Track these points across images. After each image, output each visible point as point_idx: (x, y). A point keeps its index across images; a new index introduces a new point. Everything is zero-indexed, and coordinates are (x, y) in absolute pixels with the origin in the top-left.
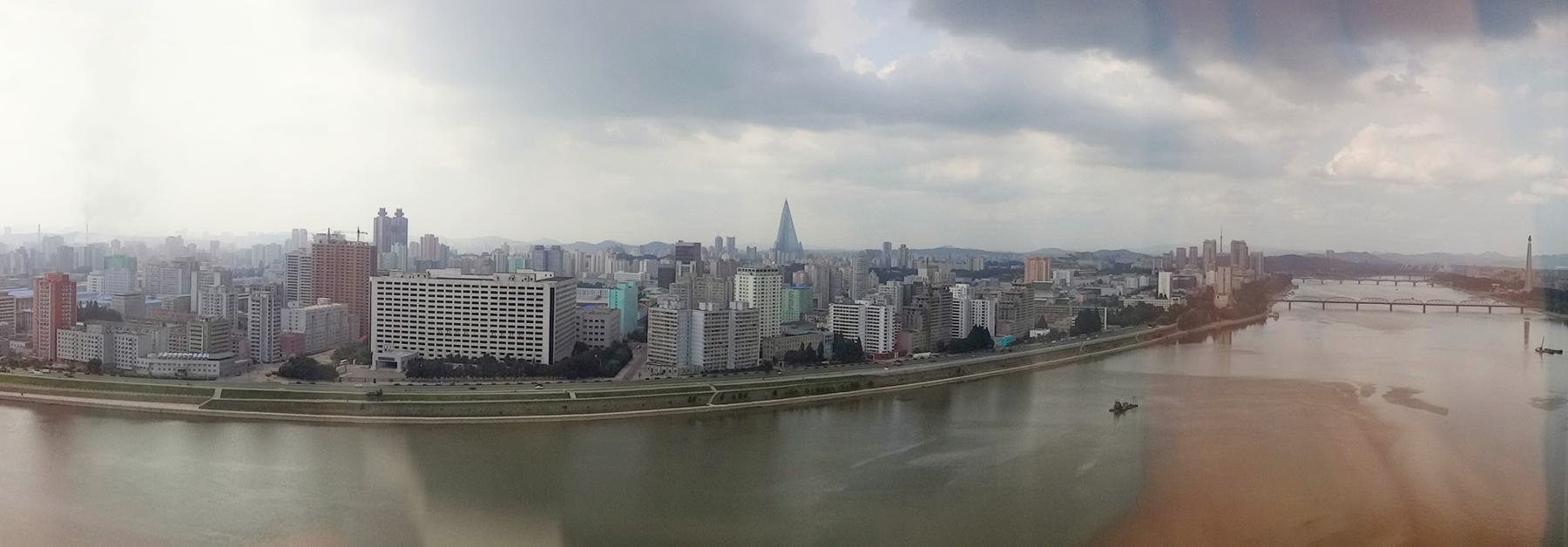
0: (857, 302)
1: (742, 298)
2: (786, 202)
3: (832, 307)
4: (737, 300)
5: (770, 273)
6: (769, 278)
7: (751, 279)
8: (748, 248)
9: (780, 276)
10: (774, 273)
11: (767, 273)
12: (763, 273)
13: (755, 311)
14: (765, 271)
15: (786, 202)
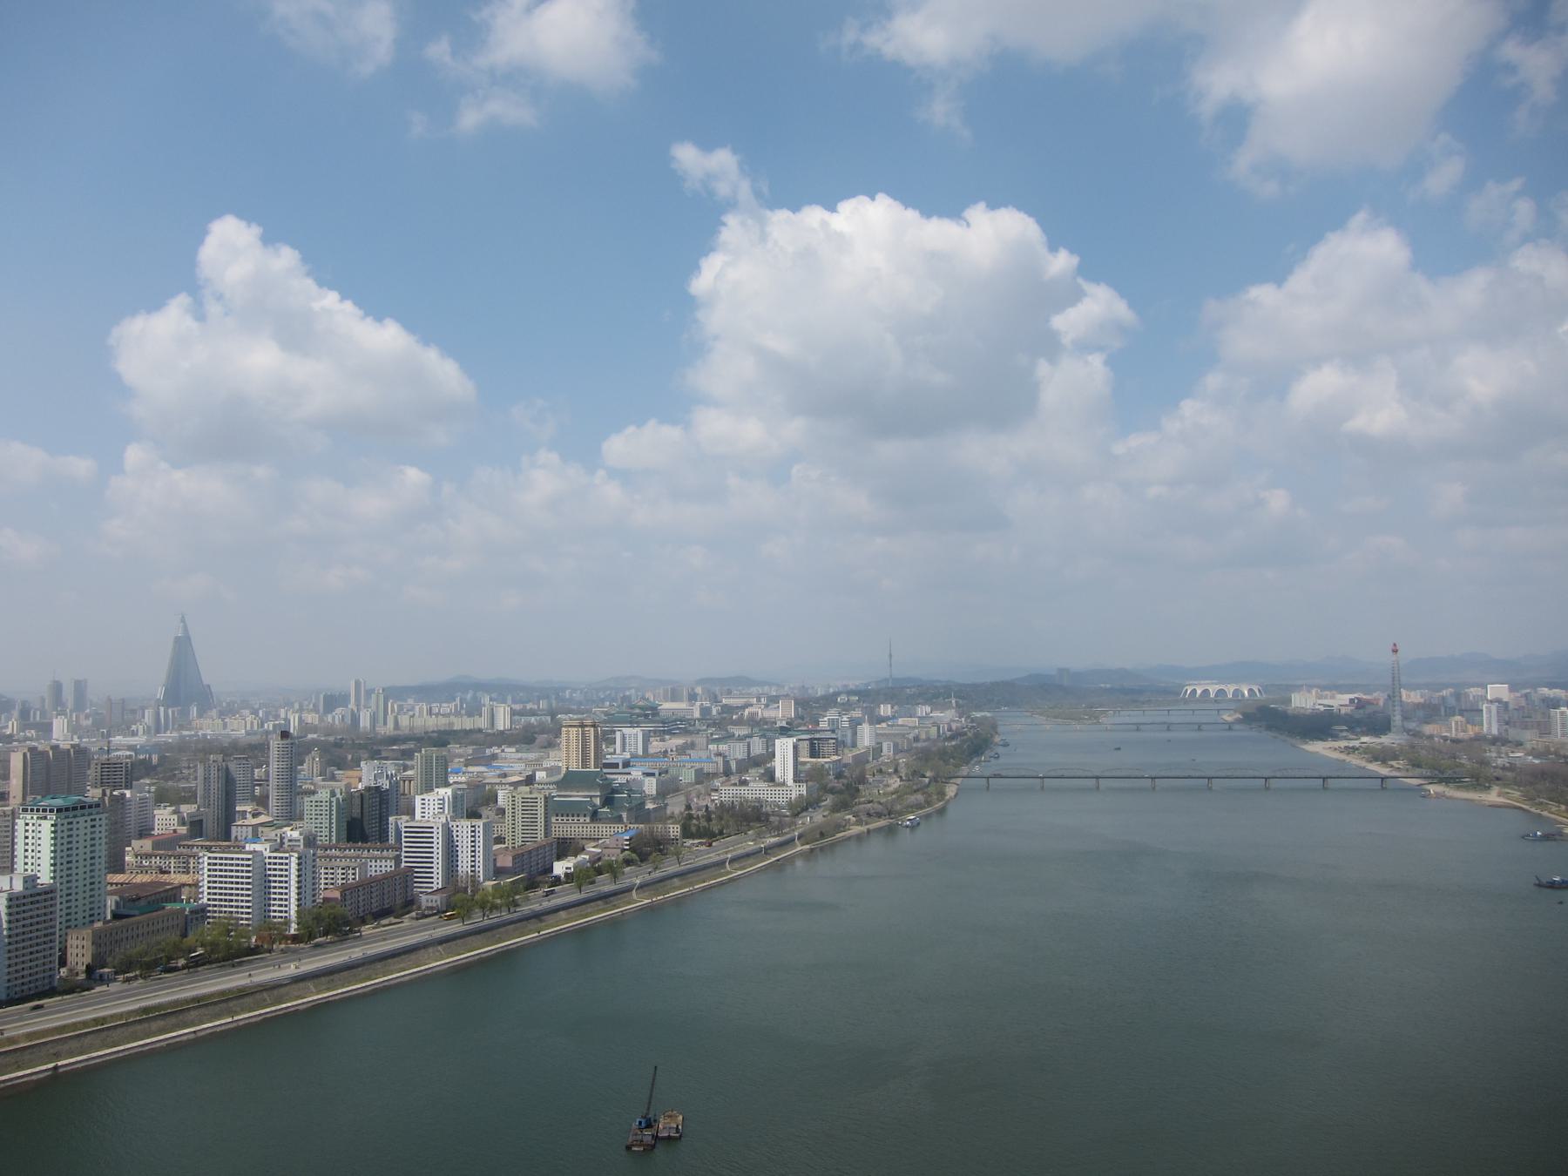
0: (249, 847)
1: (29, 867)
2: (183, 620)
3: (206, 858)
4: (19, 866)
5: (86, 811)
6: (82, 823)
7: (47, 826)
8: (109, 699)
9: (103, 816)
10: (94, 810)
11: (79, 812)
12: (71, 814)
13: (49, 892)
14: (75, 809)
15: (183, 620)
